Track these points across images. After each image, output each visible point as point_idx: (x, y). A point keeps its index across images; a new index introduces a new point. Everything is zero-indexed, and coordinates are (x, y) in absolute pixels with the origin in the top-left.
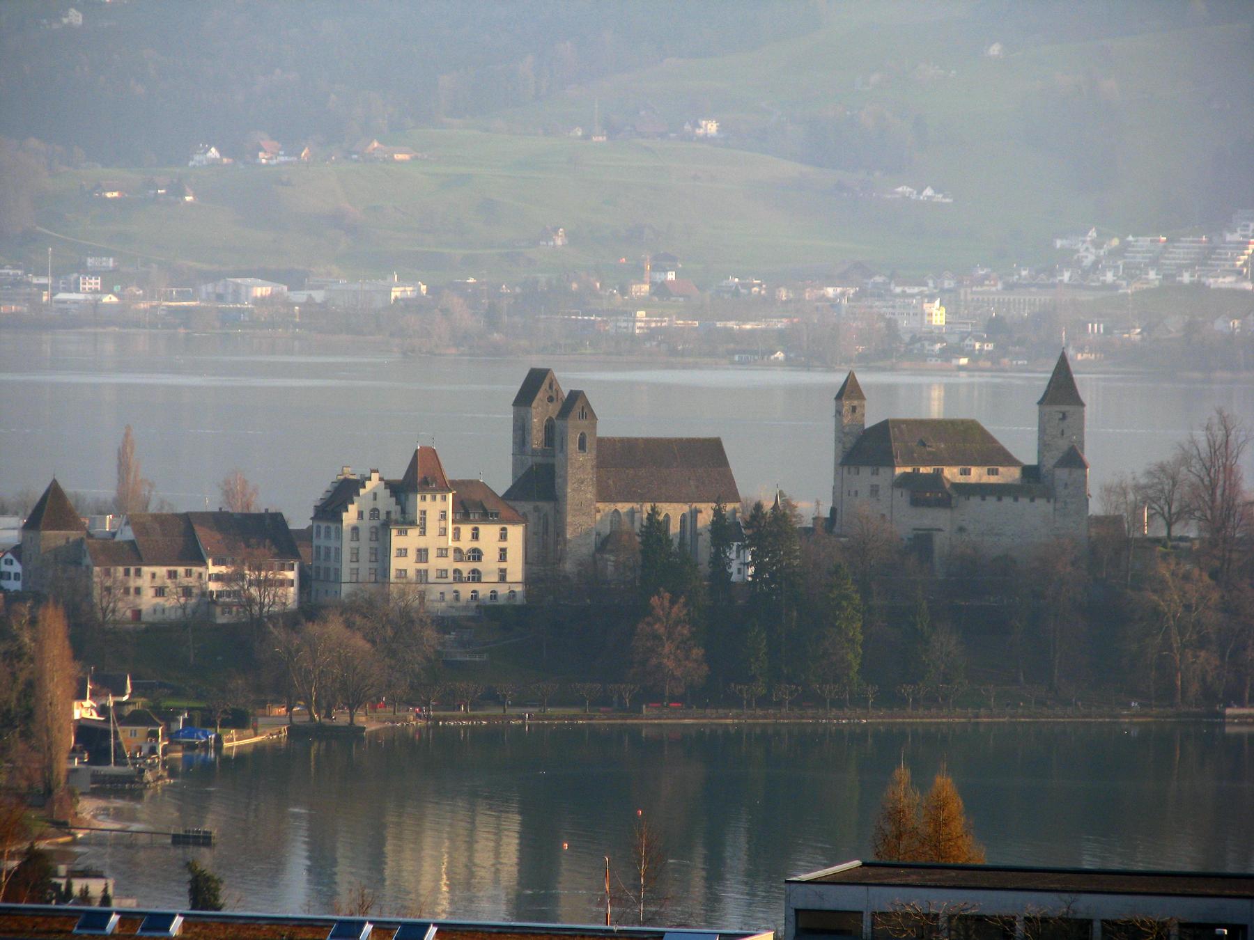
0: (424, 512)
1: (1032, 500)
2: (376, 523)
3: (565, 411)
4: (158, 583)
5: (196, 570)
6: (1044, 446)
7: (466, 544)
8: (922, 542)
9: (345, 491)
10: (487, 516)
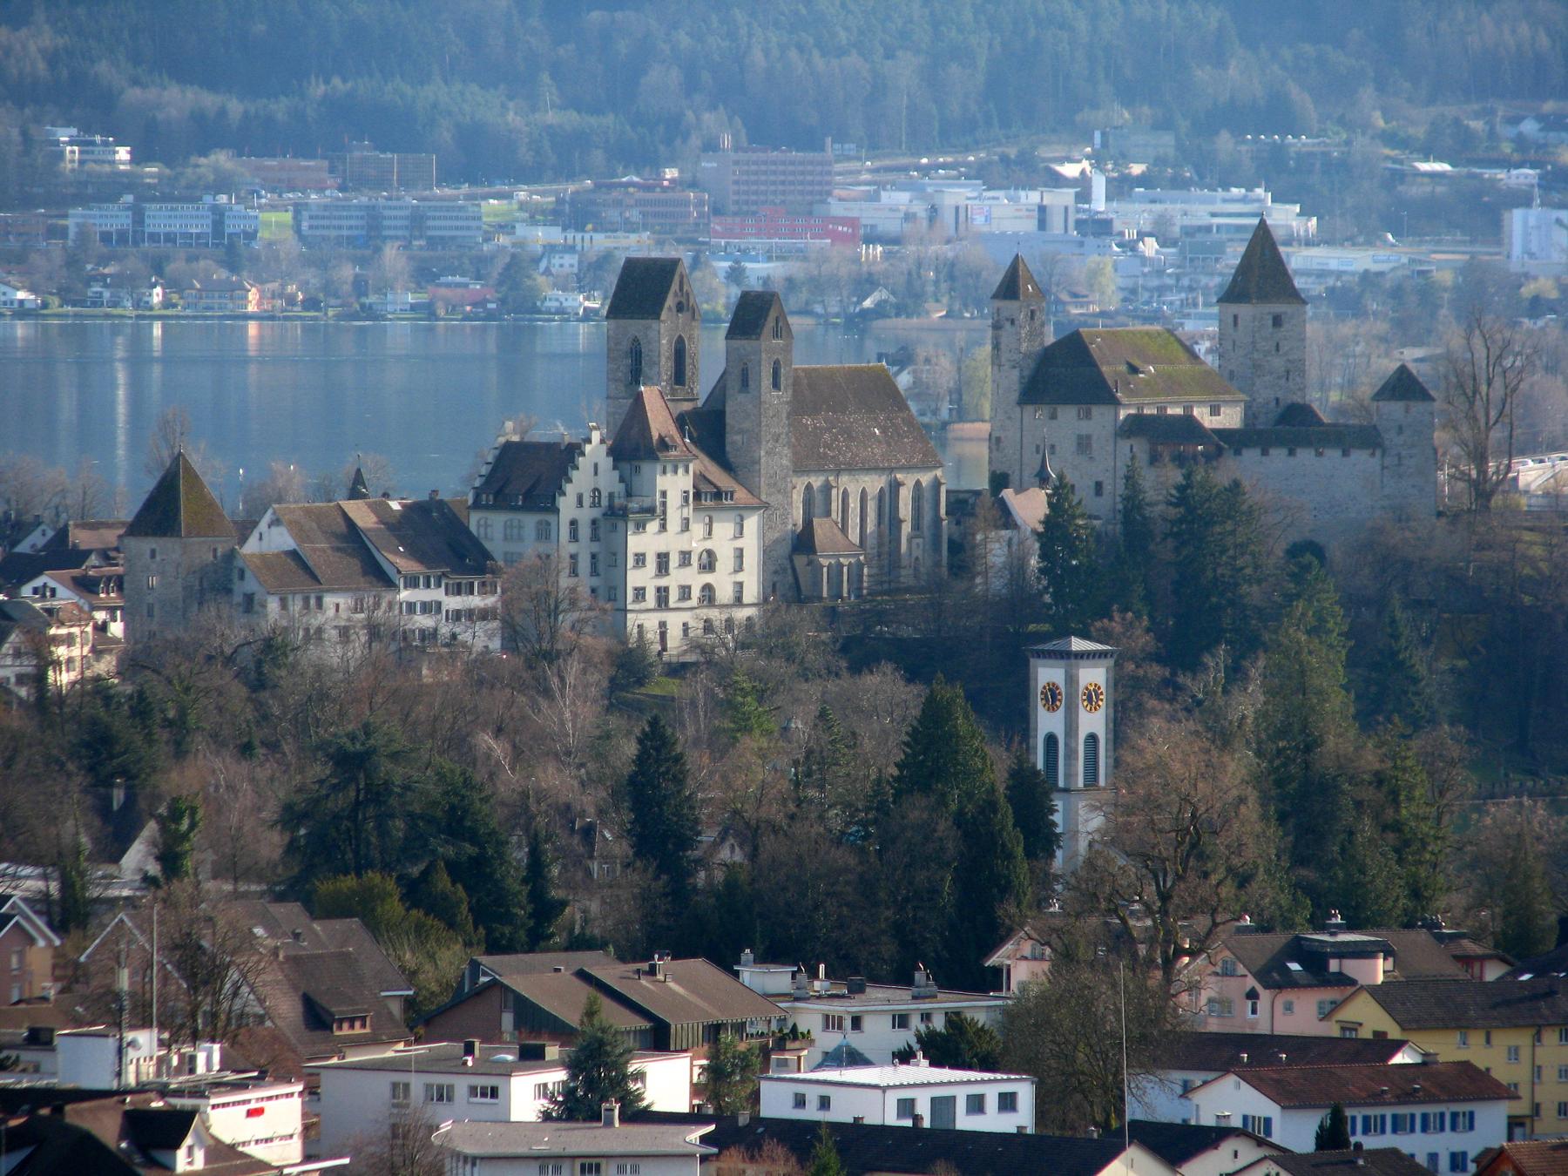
0: (664, 494)
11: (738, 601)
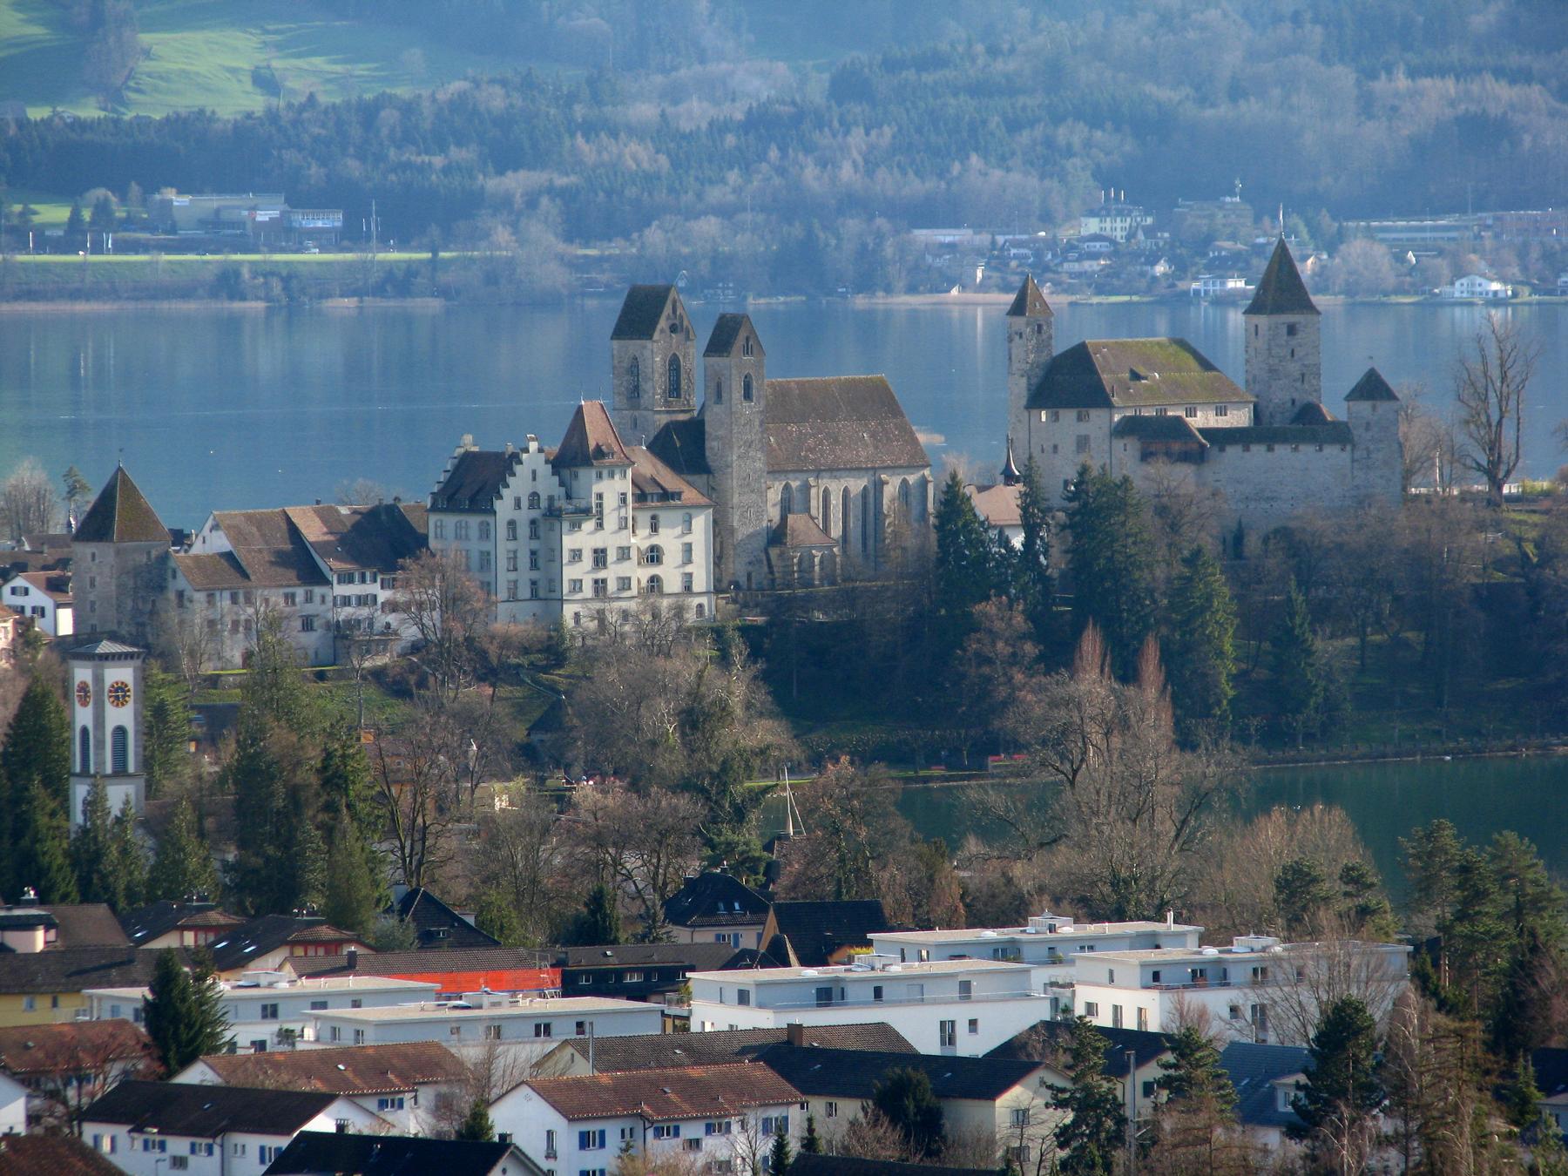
0: (600, 496)
2: (535, 514)
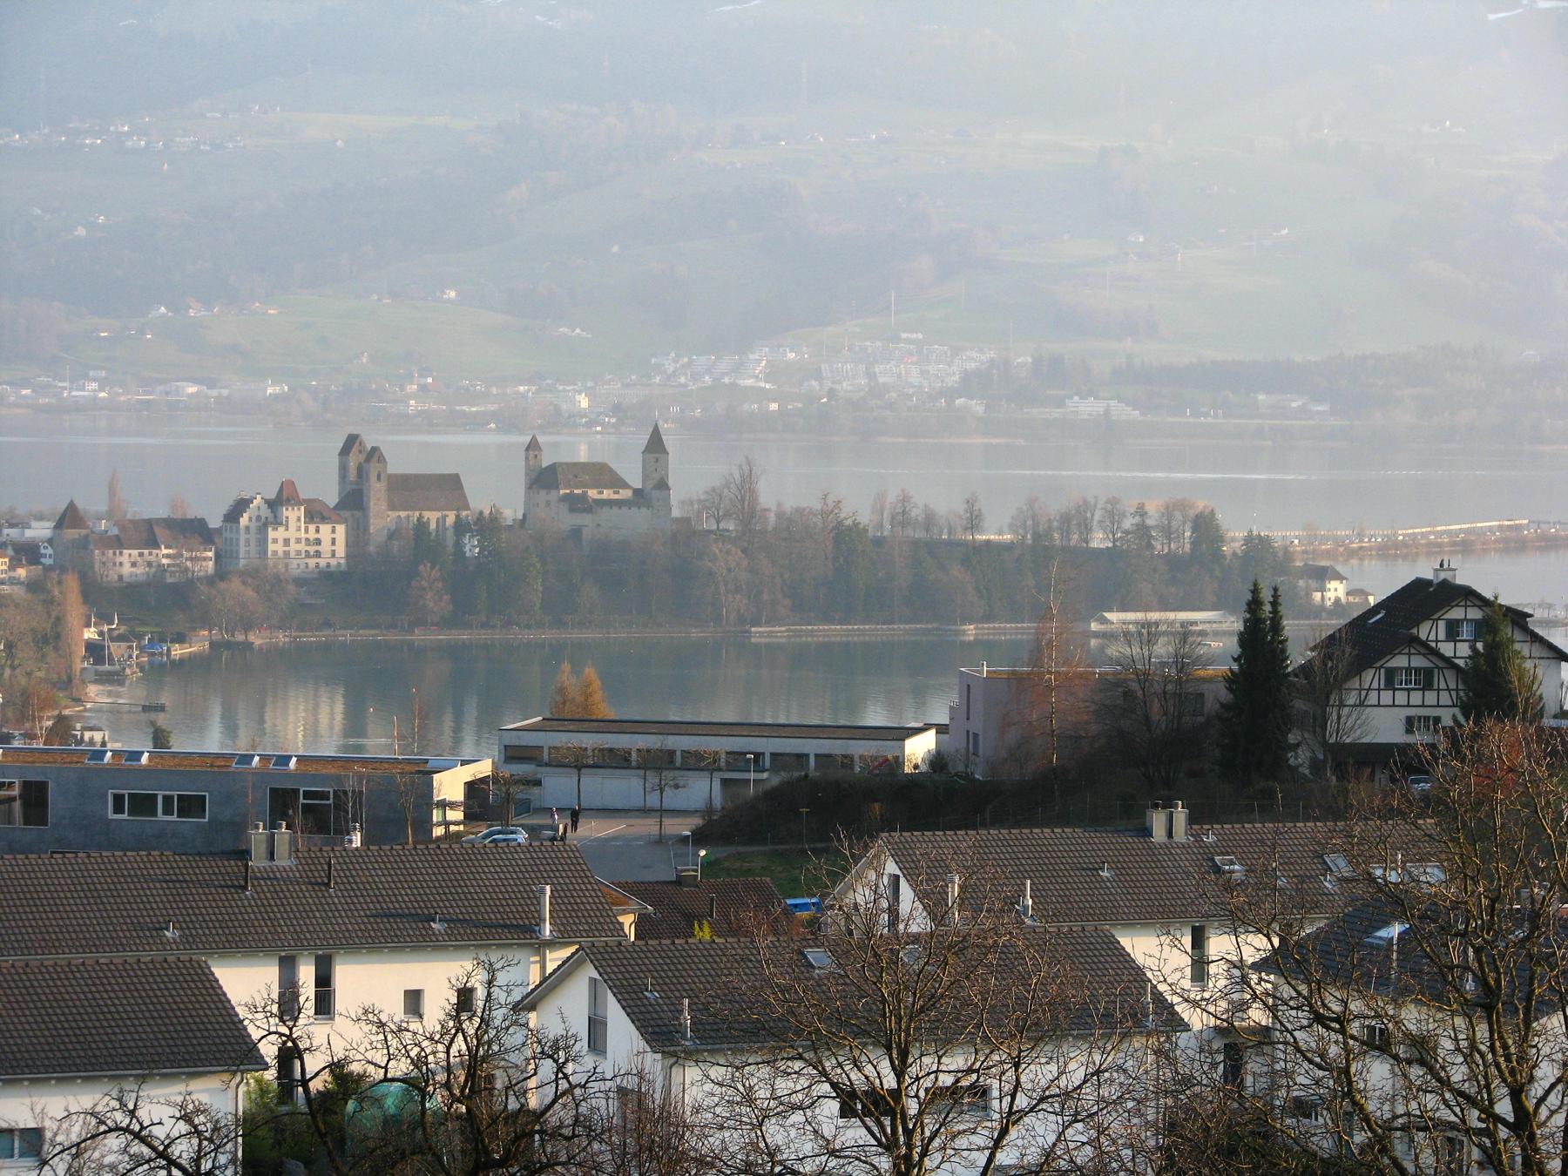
0: (287, 518)
1: (639, 508)
2: (259, 524)
3: (368, 460)
4: (133, 560)
5: (155, 551)
6: (645, 477)
7: (312, 535)
8: (576, 533)
9: (241, 505)
10: (324, 519)
11: (333, 555)
